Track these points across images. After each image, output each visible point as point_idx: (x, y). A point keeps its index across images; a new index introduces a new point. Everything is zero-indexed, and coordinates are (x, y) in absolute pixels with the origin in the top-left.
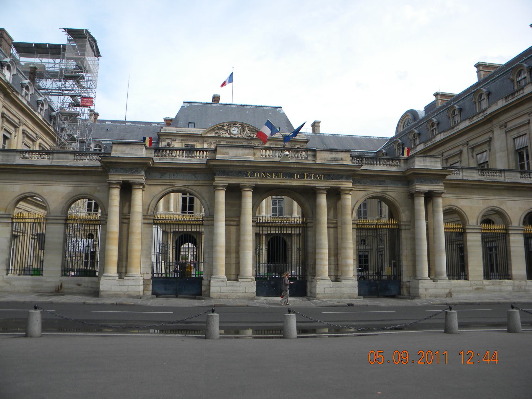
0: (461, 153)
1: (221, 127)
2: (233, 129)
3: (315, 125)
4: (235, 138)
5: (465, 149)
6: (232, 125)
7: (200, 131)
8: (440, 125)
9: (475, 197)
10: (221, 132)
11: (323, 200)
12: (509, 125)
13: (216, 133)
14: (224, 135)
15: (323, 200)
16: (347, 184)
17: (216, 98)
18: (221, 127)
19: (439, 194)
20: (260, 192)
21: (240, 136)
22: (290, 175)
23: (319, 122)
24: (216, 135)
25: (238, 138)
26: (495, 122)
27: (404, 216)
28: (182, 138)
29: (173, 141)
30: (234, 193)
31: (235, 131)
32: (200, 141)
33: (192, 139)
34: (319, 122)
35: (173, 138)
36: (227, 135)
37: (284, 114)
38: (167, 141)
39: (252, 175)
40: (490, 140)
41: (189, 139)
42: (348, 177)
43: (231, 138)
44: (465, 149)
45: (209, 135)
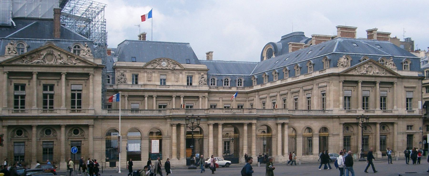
0: (299, 91)
1: (154, 61)
2: (163, 63)
3: (209, 54)
4: (164, 69)
5: (301, 90)
6: (162, 60)
8: (290, 72)
9: (301, 122)
10: (155, 65)
12: (320, 85)
13: (152, 66)
14: (157, 68)
16: (254, 122)
17: (143, 36)
18: (154, 61)
19: (288, 124)
20: (224, 125)
21: (168, 68)
23: (212, 52)
24: (153, 68)
25: (166, 69)
26: (315, 81)
27: (274, 132)
28: (130, 70)
29: (125, 71)
30: (216, 126)
32: (142, 72)
33: (137, 70)
34: (212, 52)
35: (124, 69)
36: (160, 68)
37: (191, 49)
38: (121, 71)
39: (222, 120)
40: (312, 89)
41: (134, 70)
43: (162, 69)
44: (301, 90)
45: (148, 67)
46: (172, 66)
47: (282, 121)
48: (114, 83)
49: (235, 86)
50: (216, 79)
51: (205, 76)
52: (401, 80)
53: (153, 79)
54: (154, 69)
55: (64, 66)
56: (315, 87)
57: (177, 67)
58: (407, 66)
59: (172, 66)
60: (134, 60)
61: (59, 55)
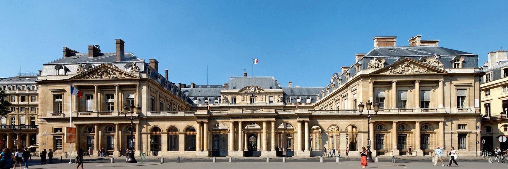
7: (237, 90)
11: (264, 125)
15: (264, 125)
22: (254, 117)
31: (253, 90)
42: (274, 117)
46: (258, 91)
47: (302, 119)
48: (220, 103)
49: (305, 102)
50: (290, 98)
51: (282, 96)
52: (449, 77)
53: (245, 99)
54: (246, 93)
55: (116, 80)
56: (349, 92)
57: (262, 91)
58: (458, 64)
59: (258, 91)
60: (234, 88)
61: (112, 72)
